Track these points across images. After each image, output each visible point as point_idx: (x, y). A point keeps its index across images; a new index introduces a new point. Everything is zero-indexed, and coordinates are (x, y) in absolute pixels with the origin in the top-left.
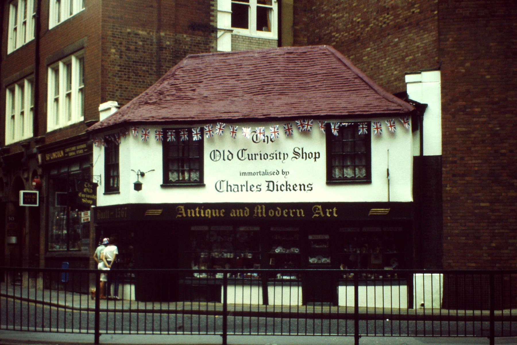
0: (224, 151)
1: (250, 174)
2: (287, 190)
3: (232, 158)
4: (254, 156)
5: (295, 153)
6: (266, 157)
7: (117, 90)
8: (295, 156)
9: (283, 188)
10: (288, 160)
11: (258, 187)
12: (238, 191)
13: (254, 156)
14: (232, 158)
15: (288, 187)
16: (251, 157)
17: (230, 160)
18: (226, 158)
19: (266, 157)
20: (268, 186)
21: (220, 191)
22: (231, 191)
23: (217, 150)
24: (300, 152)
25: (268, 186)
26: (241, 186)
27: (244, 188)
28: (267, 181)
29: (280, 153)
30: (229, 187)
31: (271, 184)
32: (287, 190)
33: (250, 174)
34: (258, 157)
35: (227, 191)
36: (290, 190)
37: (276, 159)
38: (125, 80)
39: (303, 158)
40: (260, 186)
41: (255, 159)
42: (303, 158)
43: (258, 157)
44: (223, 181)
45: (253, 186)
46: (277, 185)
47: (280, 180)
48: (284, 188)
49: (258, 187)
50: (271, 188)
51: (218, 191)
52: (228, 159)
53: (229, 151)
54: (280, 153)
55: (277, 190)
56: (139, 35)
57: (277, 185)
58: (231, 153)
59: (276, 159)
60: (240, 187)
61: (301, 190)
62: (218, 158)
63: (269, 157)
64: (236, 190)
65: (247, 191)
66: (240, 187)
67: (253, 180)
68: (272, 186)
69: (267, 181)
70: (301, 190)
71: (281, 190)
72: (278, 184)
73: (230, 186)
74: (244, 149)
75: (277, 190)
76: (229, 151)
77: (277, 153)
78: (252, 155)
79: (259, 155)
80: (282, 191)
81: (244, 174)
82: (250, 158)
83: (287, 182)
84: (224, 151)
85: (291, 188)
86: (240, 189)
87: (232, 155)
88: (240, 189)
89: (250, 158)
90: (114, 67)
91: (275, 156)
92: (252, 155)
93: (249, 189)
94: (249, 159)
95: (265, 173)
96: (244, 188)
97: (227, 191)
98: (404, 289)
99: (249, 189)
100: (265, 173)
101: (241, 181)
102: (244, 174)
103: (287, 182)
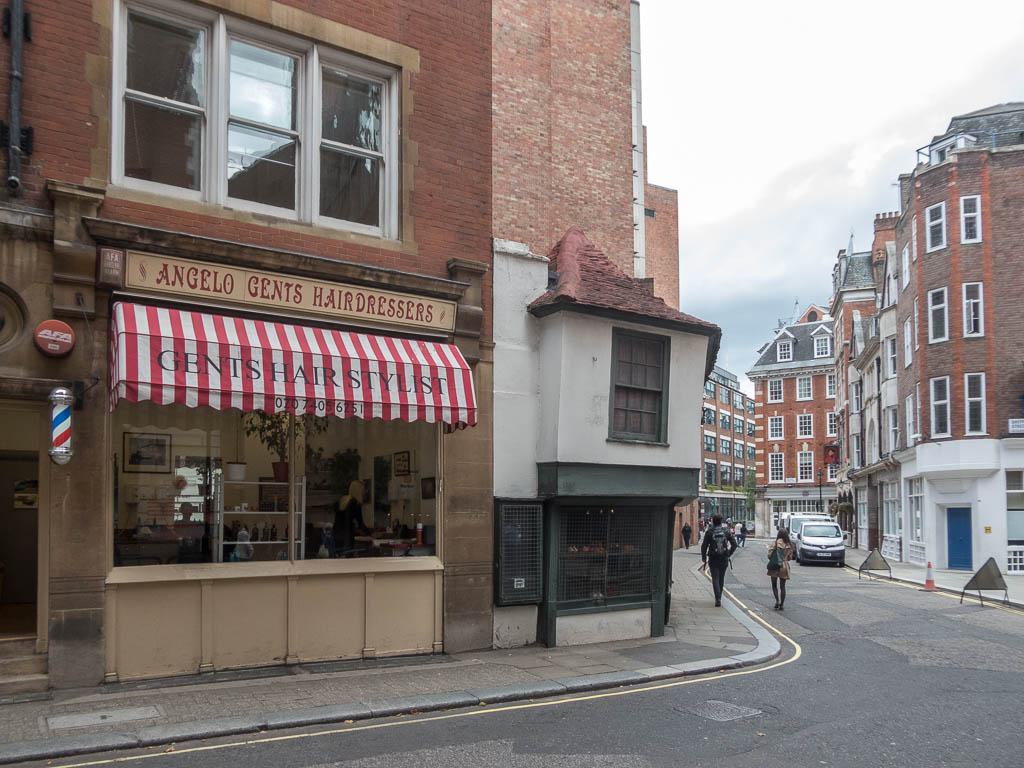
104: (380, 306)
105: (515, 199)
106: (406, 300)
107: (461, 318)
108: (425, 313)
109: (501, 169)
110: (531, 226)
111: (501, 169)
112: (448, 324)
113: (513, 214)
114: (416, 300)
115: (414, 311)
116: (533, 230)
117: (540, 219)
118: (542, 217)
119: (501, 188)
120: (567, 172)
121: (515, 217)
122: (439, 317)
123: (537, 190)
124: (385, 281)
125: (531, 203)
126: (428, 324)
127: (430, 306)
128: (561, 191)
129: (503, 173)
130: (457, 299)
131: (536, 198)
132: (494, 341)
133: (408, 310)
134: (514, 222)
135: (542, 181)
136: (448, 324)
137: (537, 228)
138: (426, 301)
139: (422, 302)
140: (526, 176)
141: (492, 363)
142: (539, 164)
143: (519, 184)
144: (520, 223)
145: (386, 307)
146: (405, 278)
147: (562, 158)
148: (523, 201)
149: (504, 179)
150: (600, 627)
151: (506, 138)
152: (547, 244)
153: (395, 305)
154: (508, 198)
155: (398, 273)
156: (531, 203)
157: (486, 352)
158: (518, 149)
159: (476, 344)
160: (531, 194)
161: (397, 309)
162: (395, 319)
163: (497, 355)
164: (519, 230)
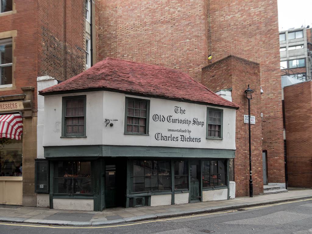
0: (160, 116)
1: (173, 130)
2: (190, 141)
3: (165, 120)
4: (175, 120)
5: (194, 121)
6: (181, 122)
7: (46, 70)
8: (194, 123)
9: (188, 140)
10: (191, 125)
11: (177, 138)
12: (167, 140)
13: (175, 120)
14: (165, 120)
15: (190, 139)
16: (174, 121)
17: (163, 121)
18: (161, 120)
19: (181, 122)
20: (181, 138)
21: (158, 139)
22: (163, 140)
23: (157, 115)
24: (196, 121)
25: (181, 138)
26: (168, 137)
27: (170, 139)
28: (181, 136)
29: (187, 120)
30: (162, 137)
31: (183, 137)
32: (190, 141)
33: (173, 130)
34: (177, 121)
35: (161, 140)
36: (191, 141)
37: (186, 123)
38: (50, 65)
39: (197, 124)
40: (178, 138)
41: (176, 122)
42: (197, 124)
43: (177, 121)
44: (159, 134)
45: (175, 138)
46: (185, 138)
47: (187, 135)
48: (188, 140)
49: (177, 138)
50: (183, 140)
51: (157, 139)
52: (162, 121)
53: (163, 116)
54: (187, 120)
55: (186, 141)
56: (55, 40)
57: (185, 138)
58: (164, 117)
59: (186, 123)
60: (168, 138)
61: (196, 141)
62: (157, 119)
63: (182, 122)
64: (166, 139)
65: (171, 140)
66: (168, 138)
67: (175, 134)
68: (183, 139)
69: (181, 136)
70: (196, 141)
71: (187, 141)
72: (186, 137)
73: (162, 136)
74: (170, 116)
75: (186, 141)
76: (163, 116)
77: (186, 120)
78: (174, 120)
79: (178, 120)
80: (188, 141)
81: (169, 130)
82: (173, 122)
83: (190, 136)
84: (160, 116)
85: (192, 140)
86: (168, 139)
87: (165, 118)
88: (168, 139)
89: (173, 122)
90: (44, 55)
91: (185, 121)
92: (174, 120)
93: (172, 139)
94: (173, 122)
95: (180, 131)
96: (170, 139)
97: (161, 140)
98: (227, 189)
99: (172, 139)
100: (180, 131)
101: (168, 134)
102: (169, 130)
103: (190, 136)
104: (4, 107)
105: (189, 40)
106: (9, 103)
107: (25, 105)
108: (15, 106)
109: (182, 31)
110: (196, 49)
111: (182, 31)
112: (22, 107)
113: (188, 46)
114: (12, 103)
115: (12, 105)
116: (197, 50)
117: (199, 45)
118: (201, 43)
119: (182, 38)
120: (240, 16)
121: (189, 47)
122: (19, 105)
123: (198, 33)
124: (3, 100)
125: (196, 39)
126: (16, 109)
127: (16, 104)
128: (237, 25)
129: (183, 32)
130: (23, 100)
131: (198, 37)
132: (38, 110)
133: (11, 106)
134: (188, 49)
135: (201, 29)
136: (22, 107)
137: (198, 48)
138: (14, 102)
139: (13, 103)
140: (193, 30)
141: (37, 116)
142: (199, 22)
143: (190, 34)
144: (190, 49)
145: (5, 106)
146: (6, 97)
147: (237, 11)
148: (192, 40)
149: (184, 34)
150: (71, 204)
151: (184, 18)
152: (203, 53)
153: (7, 106)
154: (185, 41)
155: (14, 96)
156: (196, 39)
157: (36, 113)
158: (189, 21)
159: (31, 112)
160: (196, 36)
161: (8, 106)
162: (8, 109)
163: (39, 114)
164: (191, 52)
